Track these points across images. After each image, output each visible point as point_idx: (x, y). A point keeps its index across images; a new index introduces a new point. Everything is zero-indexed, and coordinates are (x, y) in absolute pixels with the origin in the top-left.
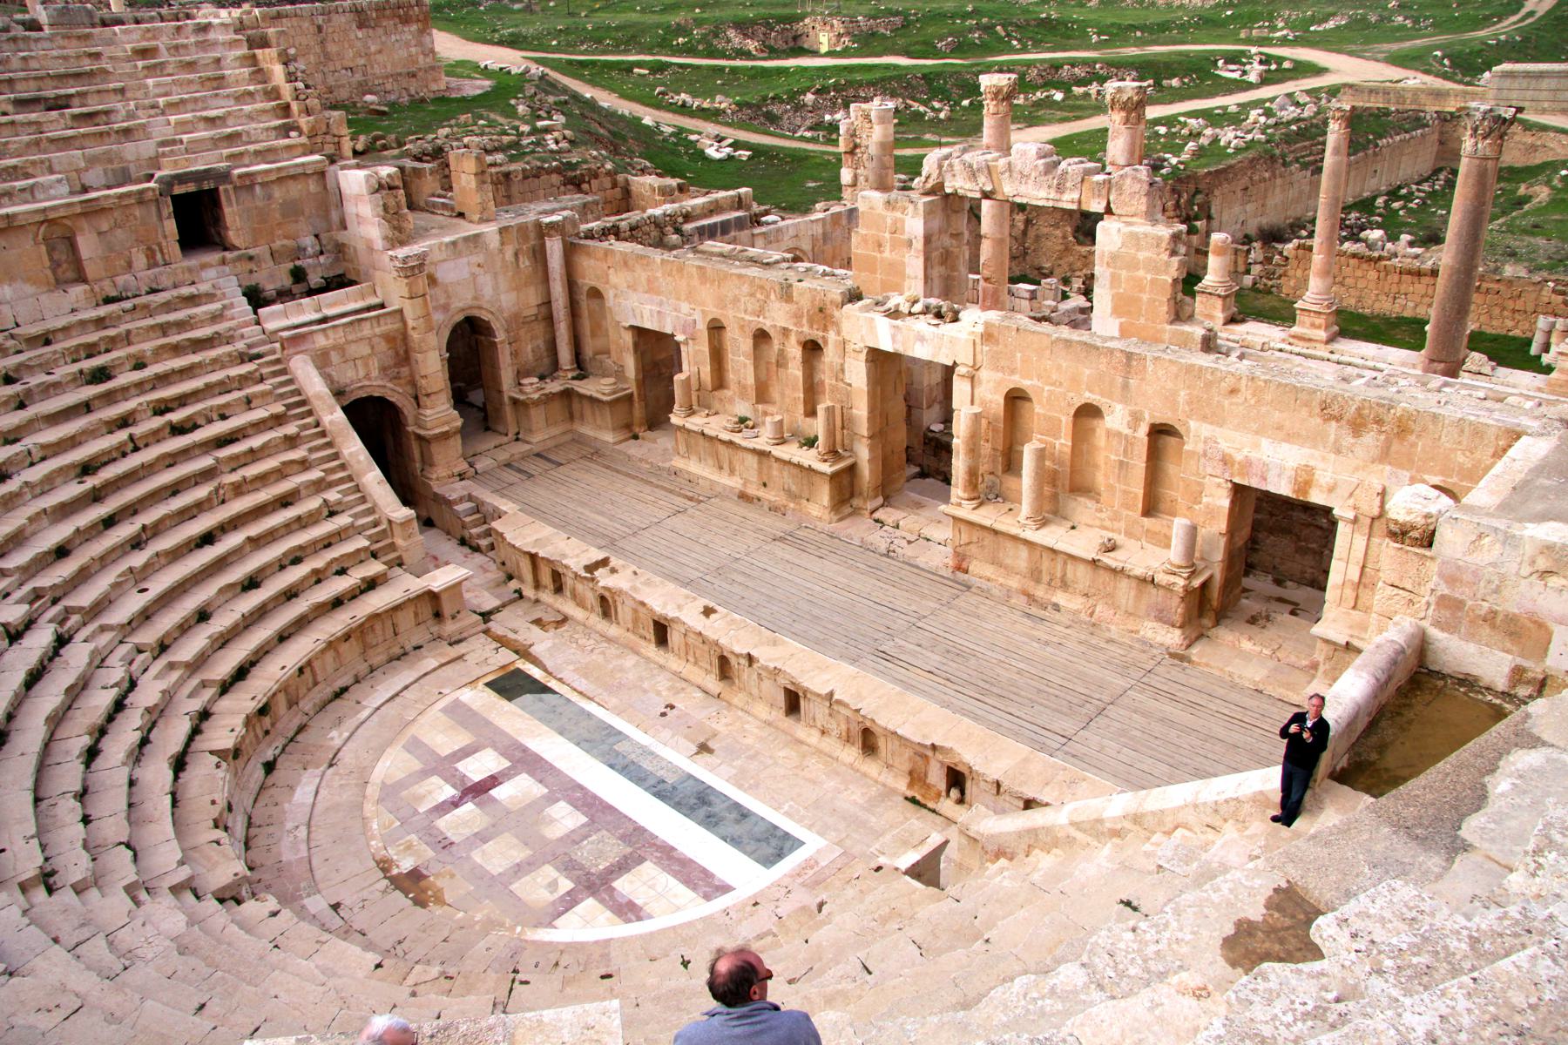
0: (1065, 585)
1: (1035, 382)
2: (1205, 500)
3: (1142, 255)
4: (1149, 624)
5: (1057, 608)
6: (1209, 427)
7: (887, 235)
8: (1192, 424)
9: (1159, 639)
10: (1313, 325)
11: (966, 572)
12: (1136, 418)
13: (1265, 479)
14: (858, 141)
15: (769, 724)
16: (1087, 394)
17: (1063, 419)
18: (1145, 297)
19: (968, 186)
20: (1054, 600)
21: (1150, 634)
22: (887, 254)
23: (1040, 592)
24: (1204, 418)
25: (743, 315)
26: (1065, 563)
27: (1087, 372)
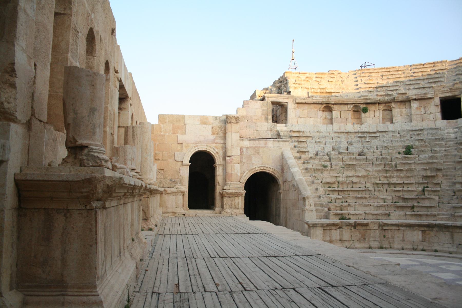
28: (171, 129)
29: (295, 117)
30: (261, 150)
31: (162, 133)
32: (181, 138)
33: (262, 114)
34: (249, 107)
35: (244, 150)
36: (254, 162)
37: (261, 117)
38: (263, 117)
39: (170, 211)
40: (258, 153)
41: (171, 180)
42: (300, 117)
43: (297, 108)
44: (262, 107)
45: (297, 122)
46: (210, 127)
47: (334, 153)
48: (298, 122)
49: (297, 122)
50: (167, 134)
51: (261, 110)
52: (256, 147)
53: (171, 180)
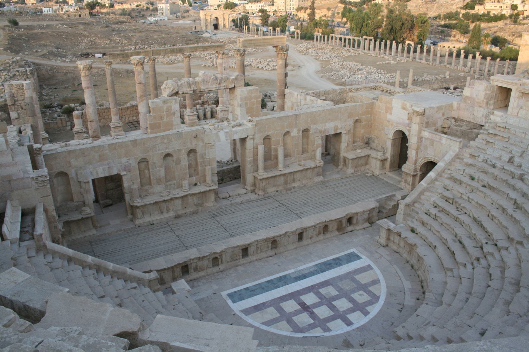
0: (294, 181)
1: (272, 132)
2: (316, 143)
3: (253, 95)
4: (315, 178)
5: (294, 187)
6: (315, 125)
7: (165, 113)
8: (312, 126)
9: (319, 180)
10: (119, 131)
11: (268, 193)
12: (299, 130)
13: (328, 132)
14: (16, 99)
15: (296, 248)
16: (286, 129)
17: (281, 139)
18: (255, 106)
19: (188, 90)
20: (293, 186)
21: (317, 180)
22: (165, 120)
23: (289, 186)
24: (314, 124)
25: (158, 152)
26: (294, 175)
27: (286, 123)
28: (385, 108)
29: (517, 107)
30: (435, 143)
31: (380, 110)
32: (389, 116)
33: (484, 98)
34: (474, 88)
35: (423, 139)
36: (429, 152)
37: (483, 101)
38: (485, 101)
39: (372, 169)
40: (433, 145)
41: (382, 147)
42: (521, 108)
43: (521, 98)
44: (485, 90)
45: (518, 113)
46: (407, 112)
47: (499, 166)
48: (519, 113)
49: (518, 113)
50: (382, 111)
51: (484, 93)
52: (432, 139)
53: (382, 147)
